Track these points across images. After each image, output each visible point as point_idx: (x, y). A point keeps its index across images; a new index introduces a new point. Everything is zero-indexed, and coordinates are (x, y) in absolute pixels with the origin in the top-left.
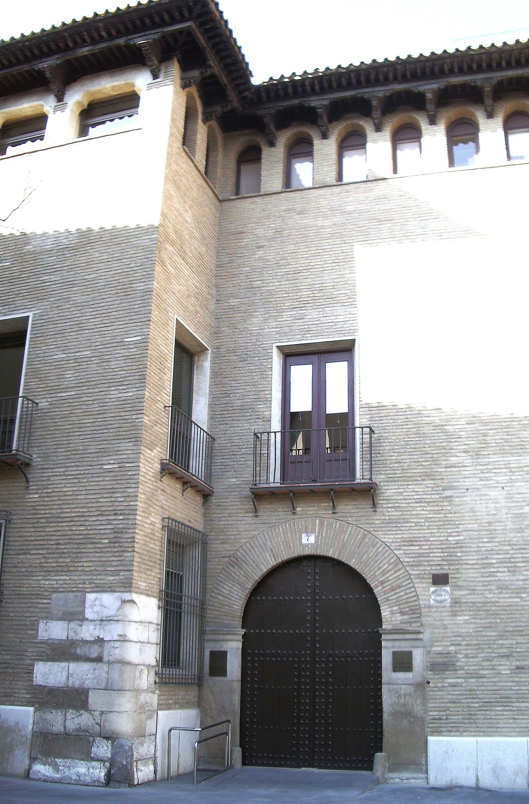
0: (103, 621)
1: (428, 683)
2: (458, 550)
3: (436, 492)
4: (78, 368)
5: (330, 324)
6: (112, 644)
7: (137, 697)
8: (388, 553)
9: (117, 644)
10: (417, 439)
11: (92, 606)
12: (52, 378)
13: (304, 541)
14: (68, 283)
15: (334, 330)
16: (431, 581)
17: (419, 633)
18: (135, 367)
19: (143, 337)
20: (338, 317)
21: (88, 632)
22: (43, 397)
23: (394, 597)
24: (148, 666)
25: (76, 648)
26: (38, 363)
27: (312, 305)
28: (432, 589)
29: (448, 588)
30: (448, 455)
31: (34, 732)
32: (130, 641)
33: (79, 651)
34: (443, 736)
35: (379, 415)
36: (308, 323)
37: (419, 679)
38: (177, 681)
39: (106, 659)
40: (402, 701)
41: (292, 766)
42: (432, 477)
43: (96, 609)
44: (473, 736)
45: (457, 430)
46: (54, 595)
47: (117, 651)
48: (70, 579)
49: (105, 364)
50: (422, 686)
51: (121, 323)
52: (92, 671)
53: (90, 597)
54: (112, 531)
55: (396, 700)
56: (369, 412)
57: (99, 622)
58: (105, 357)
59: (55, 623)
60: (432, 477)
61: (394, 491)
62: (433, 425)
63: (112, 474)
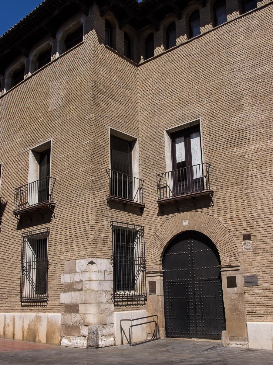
0: (83, 272)
1: (245, 293)
2: (255, 220)
3: (242, 191)
4: (68, 160)
5: (188, 114)
6: (86, 282)
7: (99, 306)
8: (221, 226)
9: (87, 282)
10: (231, 165)
11: (78, 265)
12: (60, 166)
13: (184, 224)
14: (63, 122)
15: (190, 117)
16: (242, 238)
17: (238, 266)
18: (87, 155)
19: (89, 141)
20: (191, 110)
21: (77, 278)
22: (57, 175)
23: (225, 248)
24: (106, 292)
25: (74, 285)
26: (55, 160)
27: (179, 107)
28: (243, 243)
29: (251, 242)
30: (246, 171)
31: (61, 324)
32: (93, 280)
33: (75, 287)
34: (254, 321)
35: (213, 156)
36: (178, 116)
37: (240, 291)
38: (116, 298)
39: (84, 289)
40: (233, 303)
41: (188, 338)
42: (239, 184)
43: (80, 267)
44: (270, 322)
45: (250, 157)
46: (65, 262)
47: (88, 286)
48: (70, 255)
49: (77, 156)
50: (242, 294)
51: (81, 136)
52: (79, 295)
53: (77, 261)
54: (83, 231)
55: (230, 302)
56: (208, 155)
57: (81, 273)
58: (77, 153)
59: (66, 275)
60: (239, 184)
61: (222, 193)
62: (238, 156)
63: (82, 205)
